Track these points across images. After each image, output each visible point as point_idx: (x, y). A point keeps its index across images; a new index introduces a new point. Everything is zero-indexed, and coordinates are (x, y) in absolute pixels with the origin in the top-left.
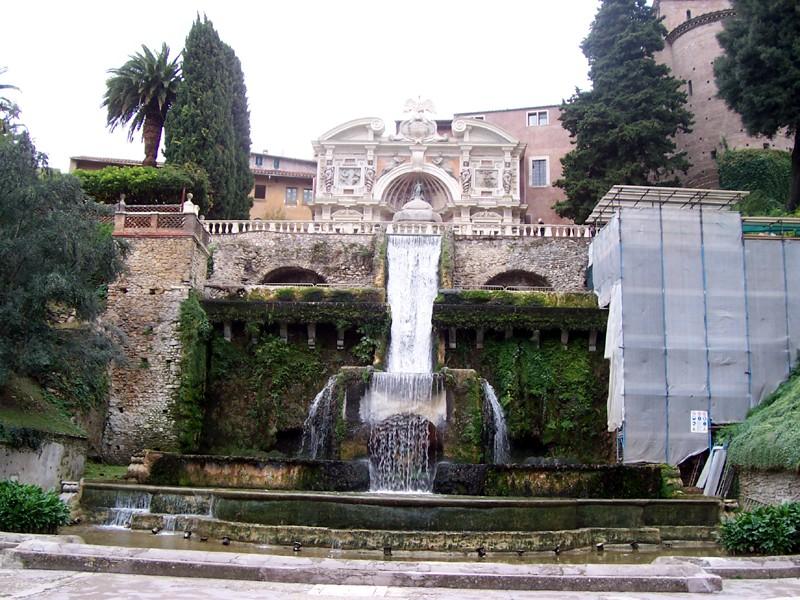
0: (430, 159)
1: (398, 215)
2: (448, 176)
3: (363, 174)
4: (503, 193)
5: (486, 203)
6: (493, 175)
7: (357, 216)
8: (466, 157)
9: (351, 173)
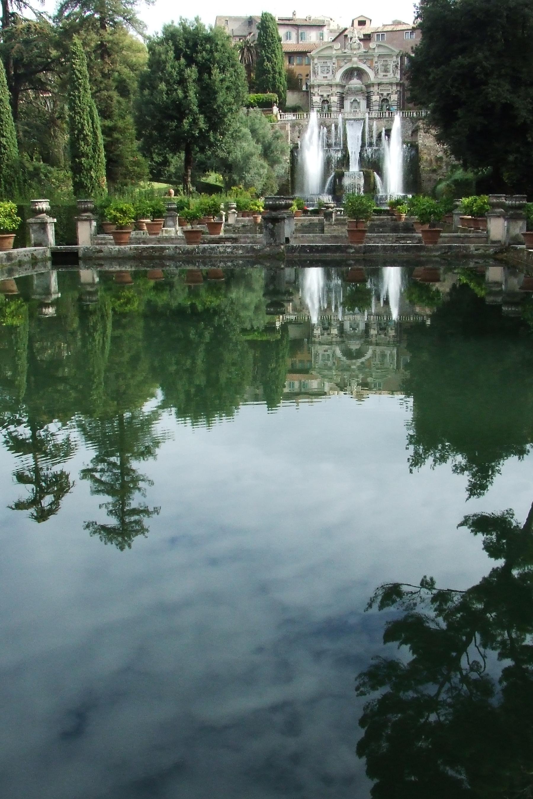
0: (360, 60)
1: (347, 86)
2: (368, 68)
3: (331, 69)
4: (392, 75)
5: (385, 80)
6: (388, 67)
7: (329, 89)
8: (376, 59)
9: (326, 68)
